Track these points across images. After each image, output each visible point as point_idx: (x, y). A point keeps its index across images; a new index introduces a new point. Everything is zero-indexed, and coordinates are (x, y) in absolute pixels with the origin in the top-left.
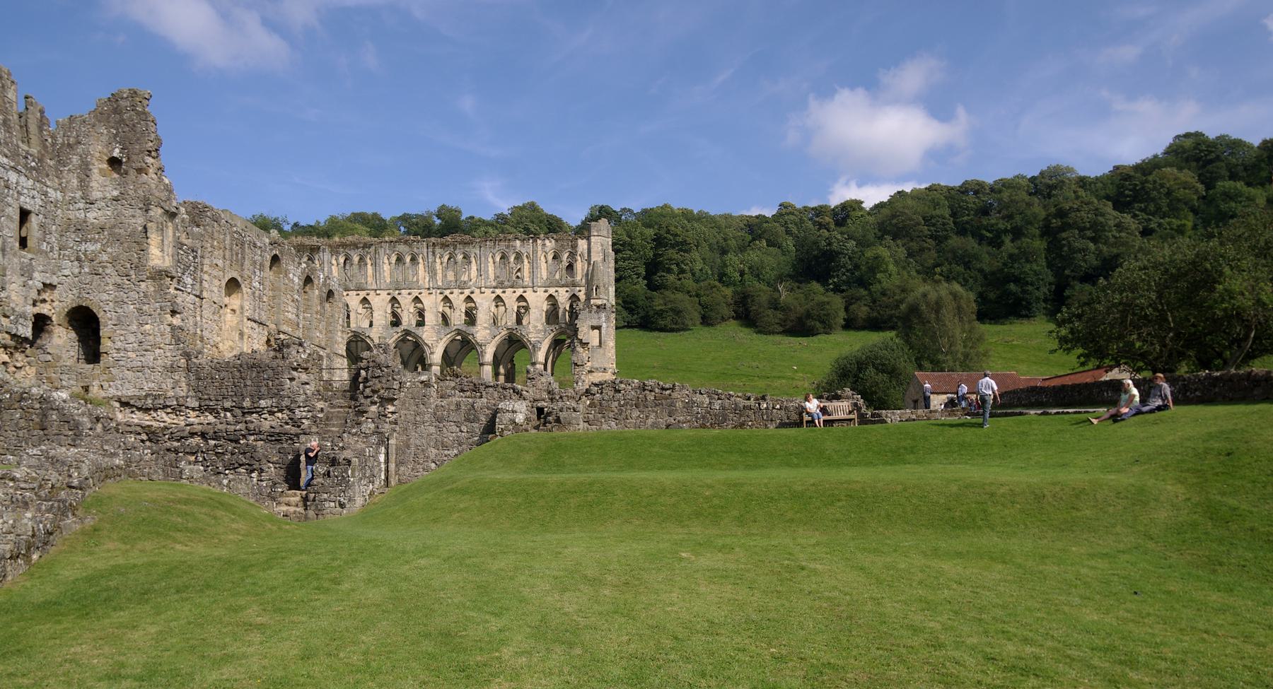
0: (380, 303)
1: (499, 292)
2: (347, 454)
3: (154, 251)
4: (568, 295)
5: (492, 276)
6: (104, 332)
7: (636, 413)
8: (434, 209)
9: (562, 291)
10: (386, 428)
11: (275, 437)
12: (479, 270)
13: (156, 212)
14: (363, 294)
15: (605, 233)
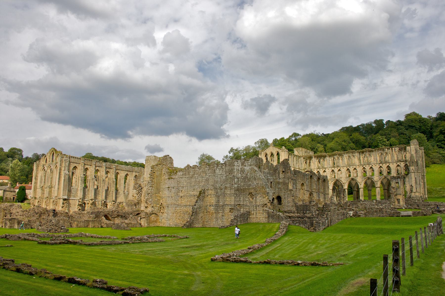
0: (344, 170)
1: (381, 165)
2: (320, 222)
3: (290, 186)
4: (404, 165)
5: (378, 160)
6: (282, 200)
7: (375, 213)
8: (373, 121)
9: (402, 163)
10: (328, 216)
11: (309, 218)
12: (374, 159)
13: (290, 180)
14: (339, 168)
15: (416, 144)
